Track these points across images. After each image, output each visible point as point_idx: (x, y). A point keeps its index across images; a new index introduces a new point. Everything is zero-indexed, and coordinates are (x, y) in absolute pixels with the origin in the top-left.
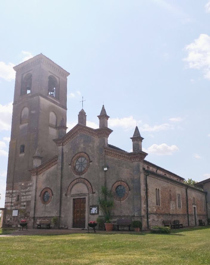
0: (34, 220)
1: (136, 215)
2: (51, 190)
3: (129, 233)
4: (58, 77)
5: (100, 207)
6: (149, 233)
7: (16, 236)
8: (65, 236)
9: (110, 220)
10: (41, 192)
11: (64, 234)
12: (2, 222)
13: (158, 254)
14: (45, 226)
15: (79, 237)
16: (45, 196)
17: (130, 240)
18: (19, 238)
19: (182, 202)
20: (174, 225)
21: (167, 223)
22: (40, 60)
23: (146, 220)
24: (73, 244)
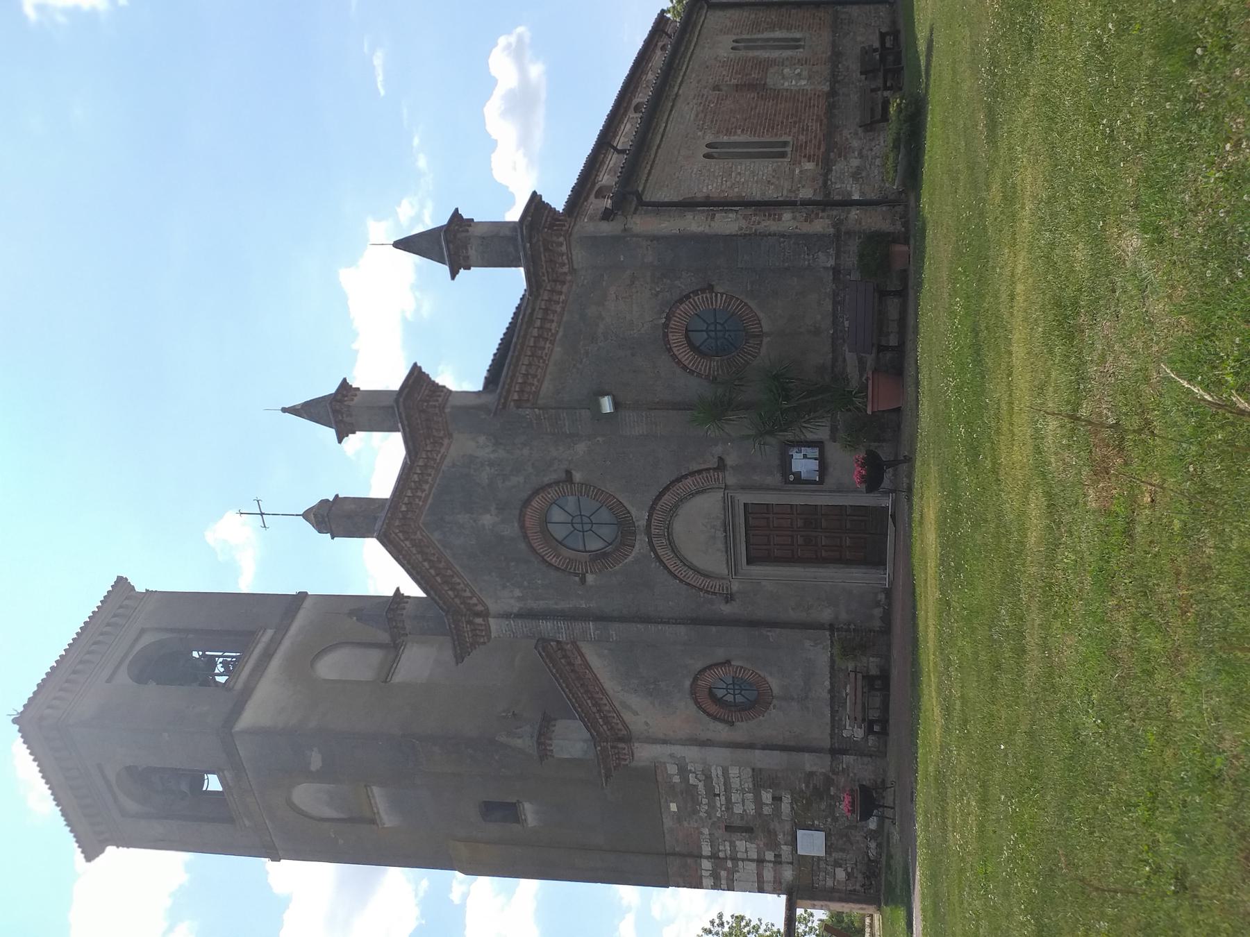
0: (844, 752)
1: (831, 263)
2: (704, 670)
3: (917, 298)
4: (136, 640)
5: (789, 436)
6: (918, 199)
7: (921, 838)
8: (921, 604)
9: (854, 384)
10: (715, 718)
11: (914, 607)
12: (852, 905)
13: (1012, 160)
14: (877, 701)
15: (928, 540)
16: (732, 701)
17: (946, 295)
18: (927, 826)
19: (772, 29)
20: (881, 74)
21: (872, 110)
22: (46, 724)
23: (854, 213)
24: (958, 569)
